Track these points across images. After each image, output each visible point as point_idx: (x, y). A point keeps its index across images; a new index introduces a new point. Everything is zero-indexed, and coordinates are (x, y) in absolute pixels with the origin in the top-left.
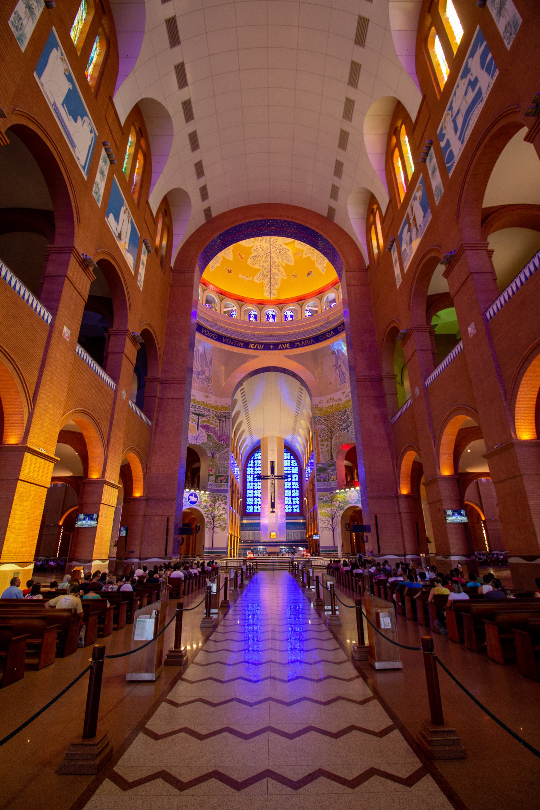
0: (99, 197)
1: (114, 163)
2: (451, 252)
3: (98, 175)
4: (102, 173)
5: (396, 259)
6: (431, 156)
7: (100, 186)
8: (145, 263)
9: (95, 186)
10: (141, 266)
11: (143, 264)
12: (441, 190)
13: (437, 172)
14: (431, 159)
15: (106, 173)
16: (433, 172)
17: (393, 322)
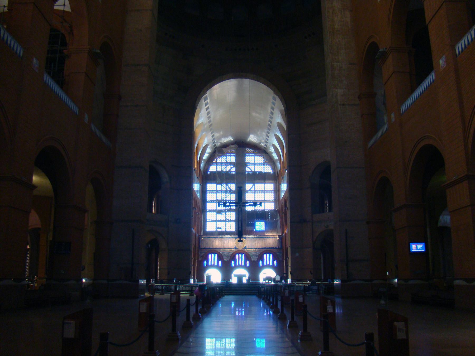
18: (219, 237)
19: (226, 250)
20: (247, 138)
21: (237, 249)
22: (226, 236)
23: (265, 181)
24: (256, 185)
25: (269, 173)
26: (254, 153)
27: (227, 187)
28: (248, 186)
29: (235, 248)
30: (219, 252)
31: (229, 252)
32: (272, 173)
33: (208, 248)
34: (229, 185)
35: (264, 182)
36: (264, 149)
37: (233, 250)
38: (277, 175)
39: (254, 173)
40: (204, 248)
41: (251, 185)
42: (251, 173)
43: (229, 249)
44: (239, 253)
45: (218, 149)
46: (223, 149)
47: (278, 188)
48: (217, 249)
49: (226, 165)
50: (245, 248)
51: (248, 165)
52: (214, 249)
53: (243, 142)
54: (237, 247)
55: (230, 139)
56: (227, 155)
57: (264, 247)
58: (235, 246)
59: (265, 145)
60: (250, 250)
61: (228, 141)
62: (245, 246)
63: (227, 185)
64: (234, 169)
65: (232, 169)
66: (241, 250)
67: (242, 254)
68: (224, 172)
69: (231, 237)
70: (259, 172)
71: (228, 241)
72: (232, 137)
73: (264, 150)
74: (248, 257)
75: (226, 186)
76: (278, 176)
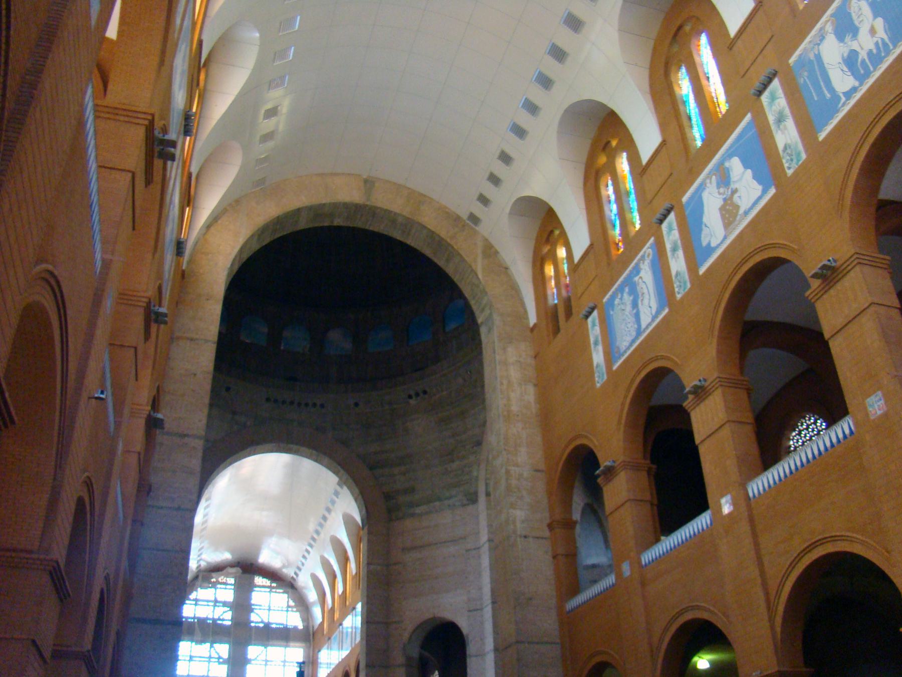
12: (685, 283)
13: (680, 253)
20: (257, 555)
23: (287, 642)
24: (269, 648)
25: (295, 628)
26: (270, 587)
27: (212, 649)
28: (253, 651)
32: (301, 626)
34: (216, 645)
35: (285, 644)
36: (292, 581)
38: (311, 629)
39: (267, 626)
41: (261, 648)
42: (261, 625)
45: (205, 573)
46: (214, 574)
47: (313, 657)
49: (215, 606)
51: (256, 609)
53: (252, 564)
55: (227, 556)
56: (219, 586)
59: (296, 574)
61: (222, 561)
63: (212, 646)
64: (228, 615)
65: (226, 616)
68: (210, 619)
70: (277, 624)
72: (228, 552)
73: (290, 582)
75: (210, 648)
76: (313, 634)
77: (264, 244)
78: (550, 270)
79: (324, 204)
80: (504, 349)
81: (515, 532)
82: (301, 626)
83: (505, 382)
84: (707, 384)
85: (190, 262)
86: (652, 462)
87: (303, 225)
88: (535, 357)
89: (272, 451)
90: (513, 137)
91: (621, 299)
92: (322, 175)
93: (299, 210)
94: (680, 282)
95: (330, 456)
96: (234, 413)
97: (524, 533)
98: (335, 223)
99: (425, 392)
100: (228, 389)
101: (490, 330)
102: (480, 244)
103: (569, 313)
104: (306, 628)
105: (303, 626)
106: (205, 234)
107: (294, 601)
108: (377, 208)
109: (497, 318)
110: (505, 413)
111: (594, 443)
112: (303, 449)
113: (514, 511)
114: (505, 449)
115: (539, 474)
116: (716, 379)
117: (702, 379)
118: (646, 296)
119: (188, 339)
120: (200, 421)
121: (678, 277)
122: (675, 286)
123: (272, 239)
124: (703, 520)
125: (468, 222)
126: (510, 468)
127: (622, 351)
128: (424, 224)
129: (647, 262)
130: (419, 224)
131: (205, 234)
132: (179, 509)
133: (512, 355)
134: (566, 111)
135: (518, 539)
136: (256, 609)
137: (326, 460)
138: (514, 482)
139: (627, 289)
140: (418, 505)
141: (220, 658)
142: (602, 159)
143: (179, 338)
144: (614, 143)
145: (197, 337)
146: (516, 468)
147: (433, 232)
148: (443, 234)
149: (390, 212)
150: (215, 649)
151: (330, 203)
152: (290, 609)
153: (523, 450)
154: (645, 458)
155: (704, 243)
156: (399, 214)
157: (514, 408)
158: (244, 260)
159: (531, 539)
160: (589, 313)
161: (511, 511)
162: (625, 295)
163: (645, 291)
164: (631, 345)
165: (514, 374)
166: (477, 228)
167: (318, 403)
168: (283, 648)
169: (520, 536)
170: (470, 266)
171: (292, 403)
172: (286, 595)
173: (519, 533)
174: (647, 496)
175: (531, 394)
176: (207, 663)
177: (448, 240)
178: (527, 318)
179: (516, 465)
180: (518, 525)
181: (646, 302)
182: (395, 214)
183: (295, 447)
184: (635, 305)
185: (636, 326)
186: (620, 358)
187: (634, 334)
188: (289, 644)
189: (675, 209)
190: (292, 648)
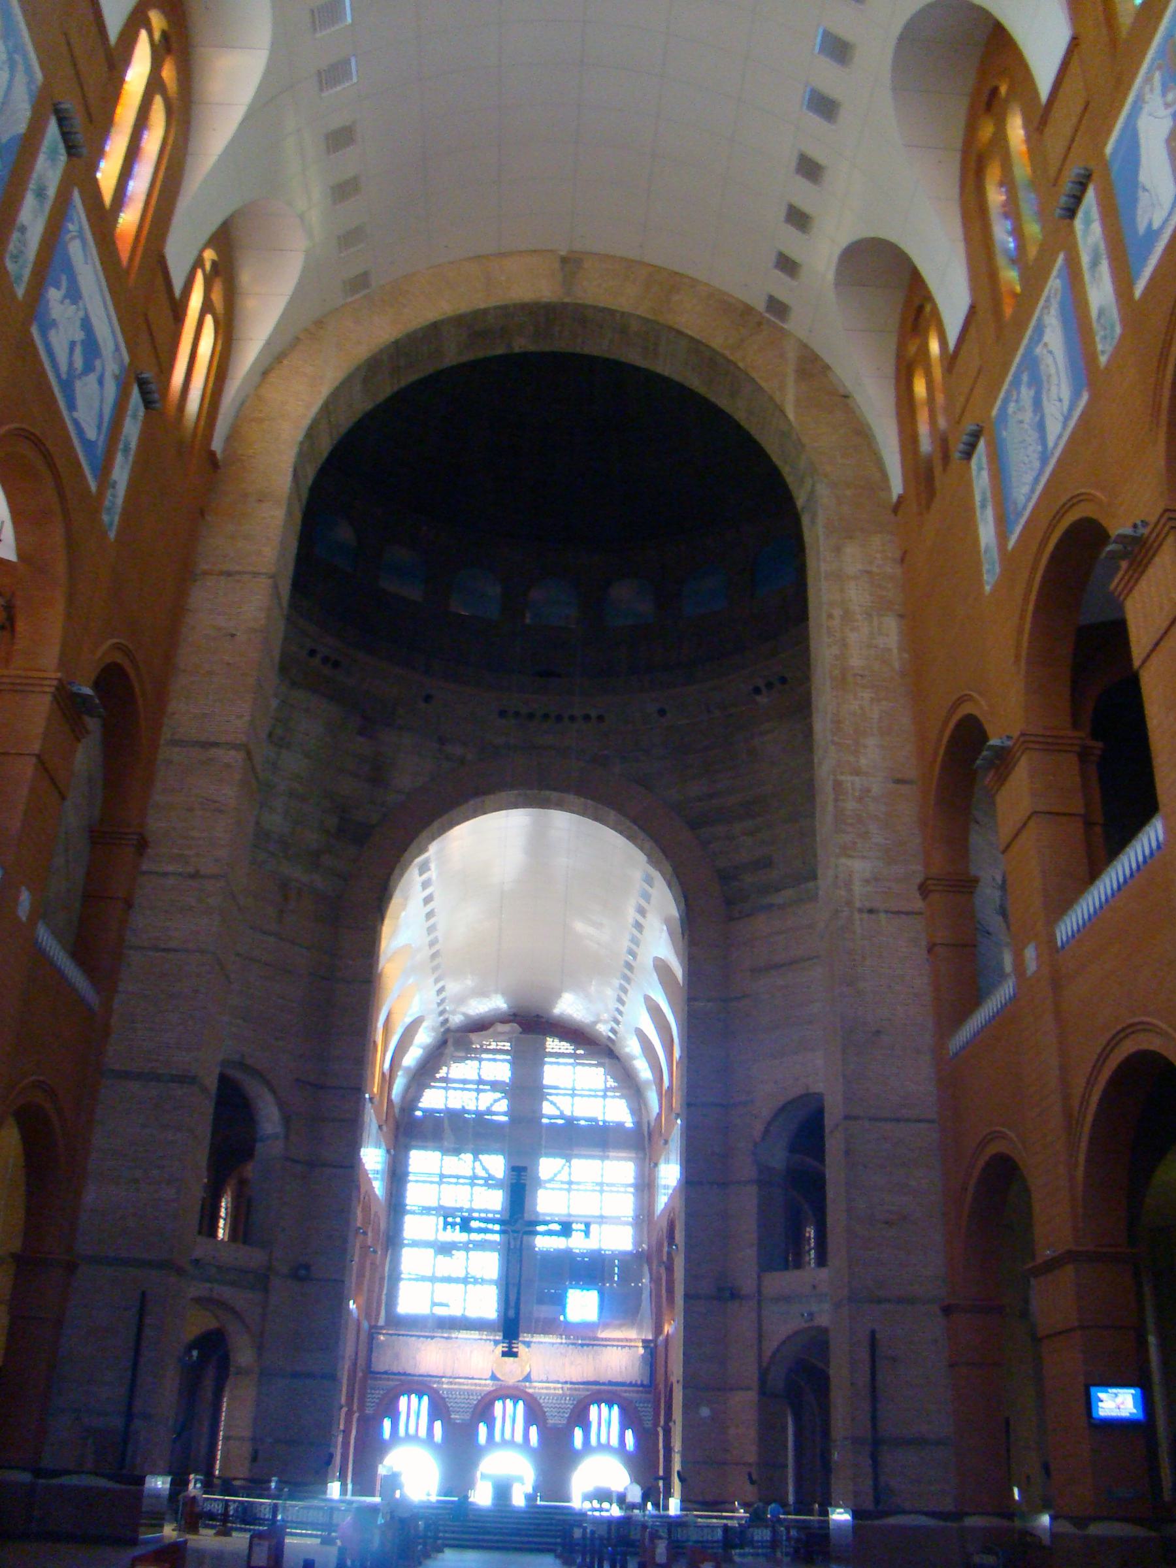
0: (22, 267)
1: (79, 156)
2: (1135, 526)
3: (30, 201)
4: (41, 194)
5: (984, 493)
6: (1087, 213)
7: (28, 234)
8: (133, 445)
9: (16, 235)
10: (119, 458)
11: (126, 450)
12: (1113, 327)
13: (1104, 267)
14: (1087, 222)
15: (51, 192)
16: (1095, 264)
17: (961, 700)
18: (439, 1335)
19: (460, 1384)
21: (500, 1383)
22: (463, 1334)
23: (604, 1151)
24: (575, 1161)
25: (620, 1126)
27: (477, 1164)
28: (548, 1166)
29: (494, 1377)
30: (436, 1391)
31: (470, 1393)
32: (629, 1124)
33: (399, 1374)
35: (601, 1153)
36: (610, 1045)
37: (485, 1385)
38: (646, 1129)
39: (571, 1122)
40: (386, 1373)
42: (561, 1122)
43: (470, 1381)
44: (503, 1398)
45: (458, 1035)
46: (473, 1037)
47: (649, 1175)
48: (429, 1379)
50: (528, 1378)
51: (550, 1094)
52: (421, 1378)
54: (499, 1376)
55: (497, 1003)
56: (484, 1056)
57: (592, 1379)
58: (493, 1373)
59: (613, 1031)
60: (542, 1388)
61: (490, 1011)
62: (525, 1373)
63: (476, 1158)
64: (503, 1106)
65: (499, 1106)
66: (516, 1388)
67: (515, 1399)
68: (469, 1112)
69: (481, 1339)
71: (471, 1352)
73: (607, 1046)
74: (535, 1413)
75: (474, 1162)
76: (650, 1134)
77: (381, 398)
78: (920, 388)
79: (485, 312)
80: (838, 549)
81: (849, 903)
82: (629, 1124)
83: (837, 612)
84: (1146, 531)
85: (231, 438)
86: (1094, 735)
87: (452, 355)
88: (902, 560)
89: (515, 805)
90: (814, 121)
91: (1017, 401)
92: (478, 258)
93: (435, 326)
94: (1105, 329)
95: (621, 810)
96: (442, 741)
97: (868, 905)
98: (517, 350)
99: (783, 680)
100: (428, 698)
101: (813, 521)
102: (792, 355)
103: (946, 457)
104: (638, 1124)
105: (633, 1123)
106: (258, 386)
107: (615, 1079)
108: (584, 306)
109: (823, 490)
110: (836, 672)
111: (978, 708)
112: (571, 798)
113: (849, 862)
114: (833, 742)
115: (905, 789)
116: (1162, 516)
117: (1139, 522)
118: (1054, 380)
119: (221, 573)
120: (240, 717)
121: (1102, 321)
122: (1098, 339)
123: (396, 388)
124: (1153, 833)
125: (767, 315)
126: (843, 778)
127: (1020, 506)
128: (676, 326)
129: (1054, 310)
130: (670, 328)
131: (258, 386)
132: (195, 876)
133: (853, 558)
134: (901, 39)
135: (857, 916)
136: (550, 1094)
137: (612, 815)
138: (850, 805)
139: (1025, 378)
140: (778, 890)
141: (491, 1177)
142: (987, 131)
143: (205, 573)
144: (1003, 90)
145: (238, 568)
146: (857, 779)
147: (698, 342)
148: (717, 343)
149: (612, 312)
150: (481, 1163)
151: (495, 308)
152: (609, 1094)
153: (871, 742)
154: (1075, 726)
155: (1142, 228)
156: (630, 315)
157: (856, 661)
158: (343, 430)
159: (883, 916)
160: (972, 446)
161: (843, 860)
162: (1024, 389)
163: (1053, 371)
164: (1032, 491)
165: (857, 595)
166: (785, 326)
167: (594, 714)
168: (597, 1162)
169: (860, 911)
170: (771, 399)
171: (546, 716)
172: (601, 1070)
173: (858, 904)
174: (1077, 805)
175: (891, 633)
176: (469, 1187)
177: (727, 353)
178: (887, 488)
179: (857, 772)
180: (857, 888)
181: (1054, 390)
182: (623, 313)
183: (554, 795)
184: (1037, 405)
185: (1040, 448)
186: (1016, 521)
187: (1037, 464)
188: (607, 1154)
189: (1095, 176)
190: (615, 1163)
